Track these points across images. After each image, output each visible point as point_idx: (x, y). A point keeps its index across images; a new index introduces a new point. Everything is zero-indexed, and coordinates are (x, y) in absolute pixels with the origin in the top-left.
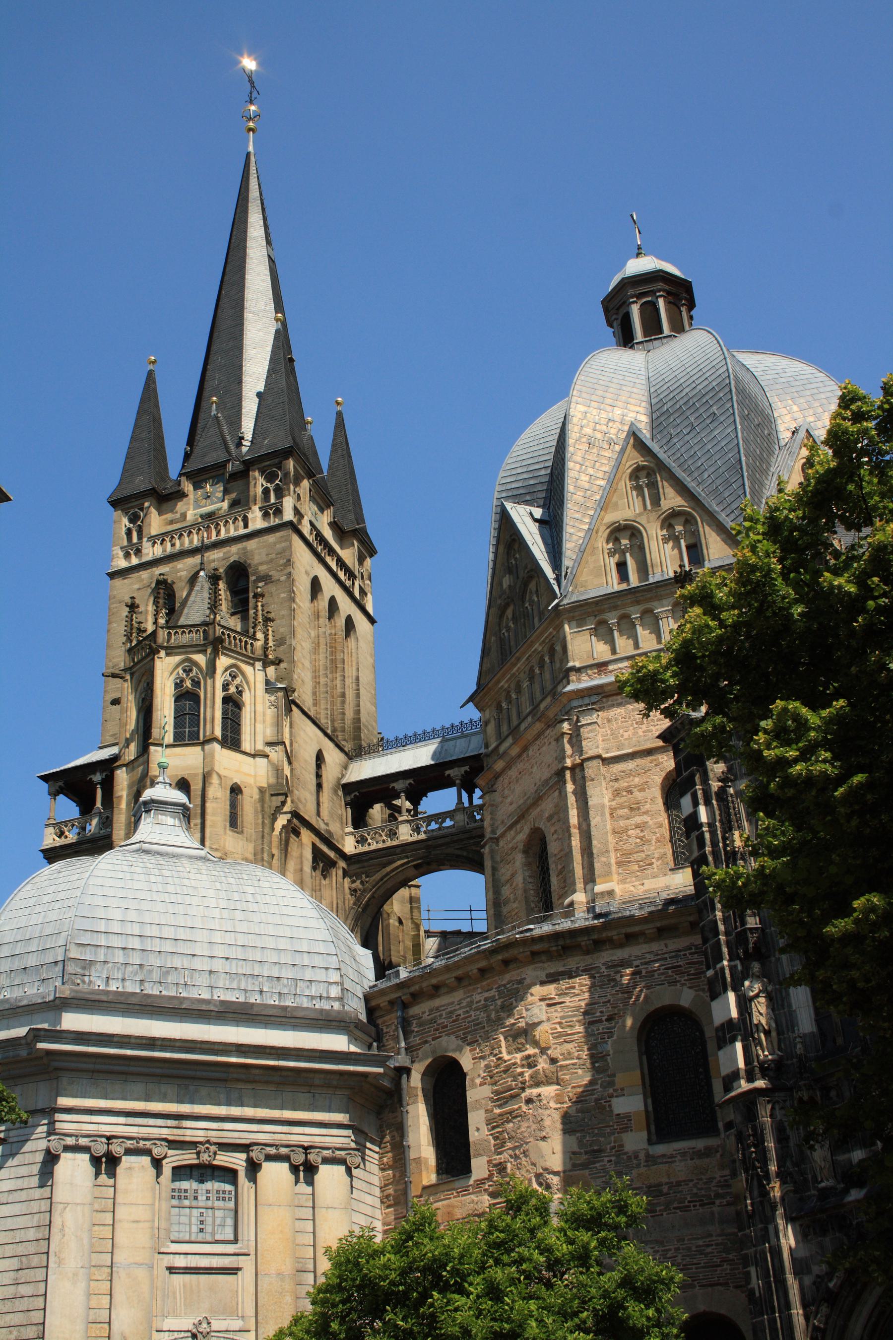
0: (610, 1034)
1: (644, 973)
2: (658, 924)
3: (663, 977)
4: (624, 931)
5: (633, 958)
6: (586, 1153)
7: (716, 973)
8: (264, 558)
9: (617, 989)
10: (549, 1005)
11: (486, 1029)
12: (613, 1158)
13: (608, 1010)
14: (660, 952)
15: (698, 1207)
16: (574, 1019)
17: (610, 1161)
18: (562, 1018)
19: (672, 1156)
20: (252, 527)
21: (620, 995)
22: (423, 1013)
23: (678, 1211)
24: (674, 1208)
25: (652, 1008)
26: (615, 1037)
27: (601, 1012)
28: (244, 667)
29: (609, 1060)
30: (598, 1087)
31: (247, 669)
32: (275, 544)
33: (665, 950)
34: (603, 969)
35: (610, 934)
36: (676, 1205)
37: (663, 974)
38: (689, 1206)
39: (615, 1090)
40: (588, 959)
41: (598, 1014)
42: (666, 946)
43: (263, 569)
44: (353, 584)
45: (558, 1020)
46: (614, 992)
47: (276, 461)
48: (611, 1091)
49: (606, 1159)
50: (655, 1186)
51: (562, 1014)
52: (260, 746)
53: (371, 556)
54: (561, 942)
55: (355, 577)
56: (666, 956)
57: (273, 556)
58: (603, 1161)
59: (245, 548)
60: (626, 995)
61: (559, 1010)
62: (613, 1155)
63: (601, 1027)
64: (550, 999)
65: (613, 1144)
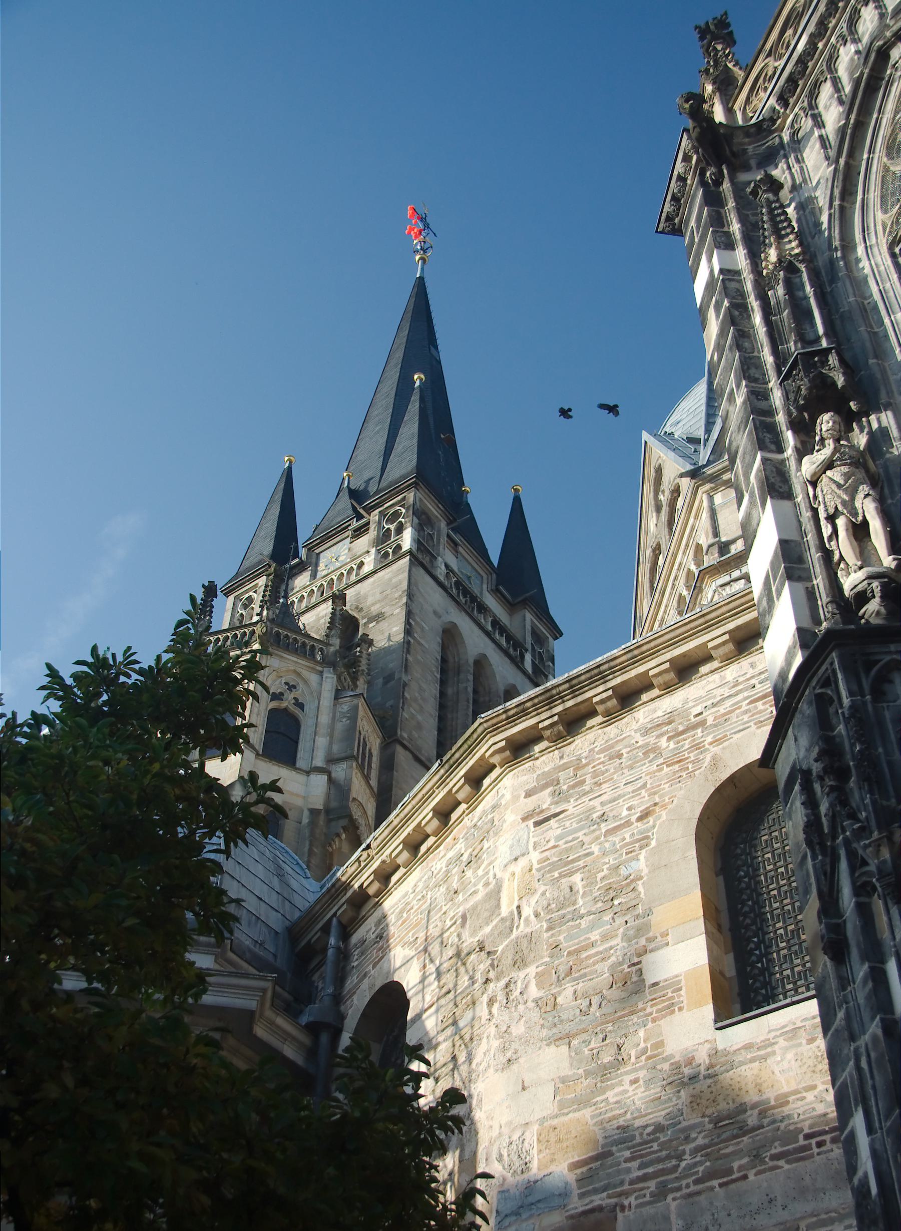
0: (645, 840)
1: (710, 721)
2: (731, 626)
3: (746, 718)
4: (668, 656)
5: (691, 704)
6: (587, 1074)
7: (752, 496)
8: (378, 596)
9: (661, 761)
10: (537, 824)
11: (444, 909)
12: (642, 1074)
13: (642, 802)
14: (741, 679)
15: (828, 1146)
16: (580, 834)
17: (634, 1082)
18: (559, 838)
19: (770, 1044)
20: (367, 569)
21: (666, 770)
22: (367, 932)
23: (781, 1163)
24: (774, 1157)
25: (725, 775)
26: (653, 843)
27: (629, 809)
28: (306, 673)
29: (641, 889)
30: (617, 940)
31: (313, 678)
32: (390, 579)
33: (751, 672)
34: (637, 737)
35: (641, 669)
36: (777, 1149)
37: (746, 712)
38: (808, 1148)
39: (649, 940)
40: (612, 730)
41: (625, 813)
42: (752, 665)
43: (375, 610)
44: (522, 657)
45: (551, 844)
46: (655, 767)
47: (399, 498)
48: (643, 941)
49: (627, 1079)
50: (729, 1117)
51: (559, 831)
52: (319, 762)
53: (556, 638)
54: (559, 708)
55: (526, 650)
56: (753, 681)
57: (388, 592)
58: (620, 1083)
59: (359, 593)
60: (676, 767)
61: (556, 825)
62: (641, 1068)
63: (627, 834)
64: (542, 811)
65: (642, 1045)
